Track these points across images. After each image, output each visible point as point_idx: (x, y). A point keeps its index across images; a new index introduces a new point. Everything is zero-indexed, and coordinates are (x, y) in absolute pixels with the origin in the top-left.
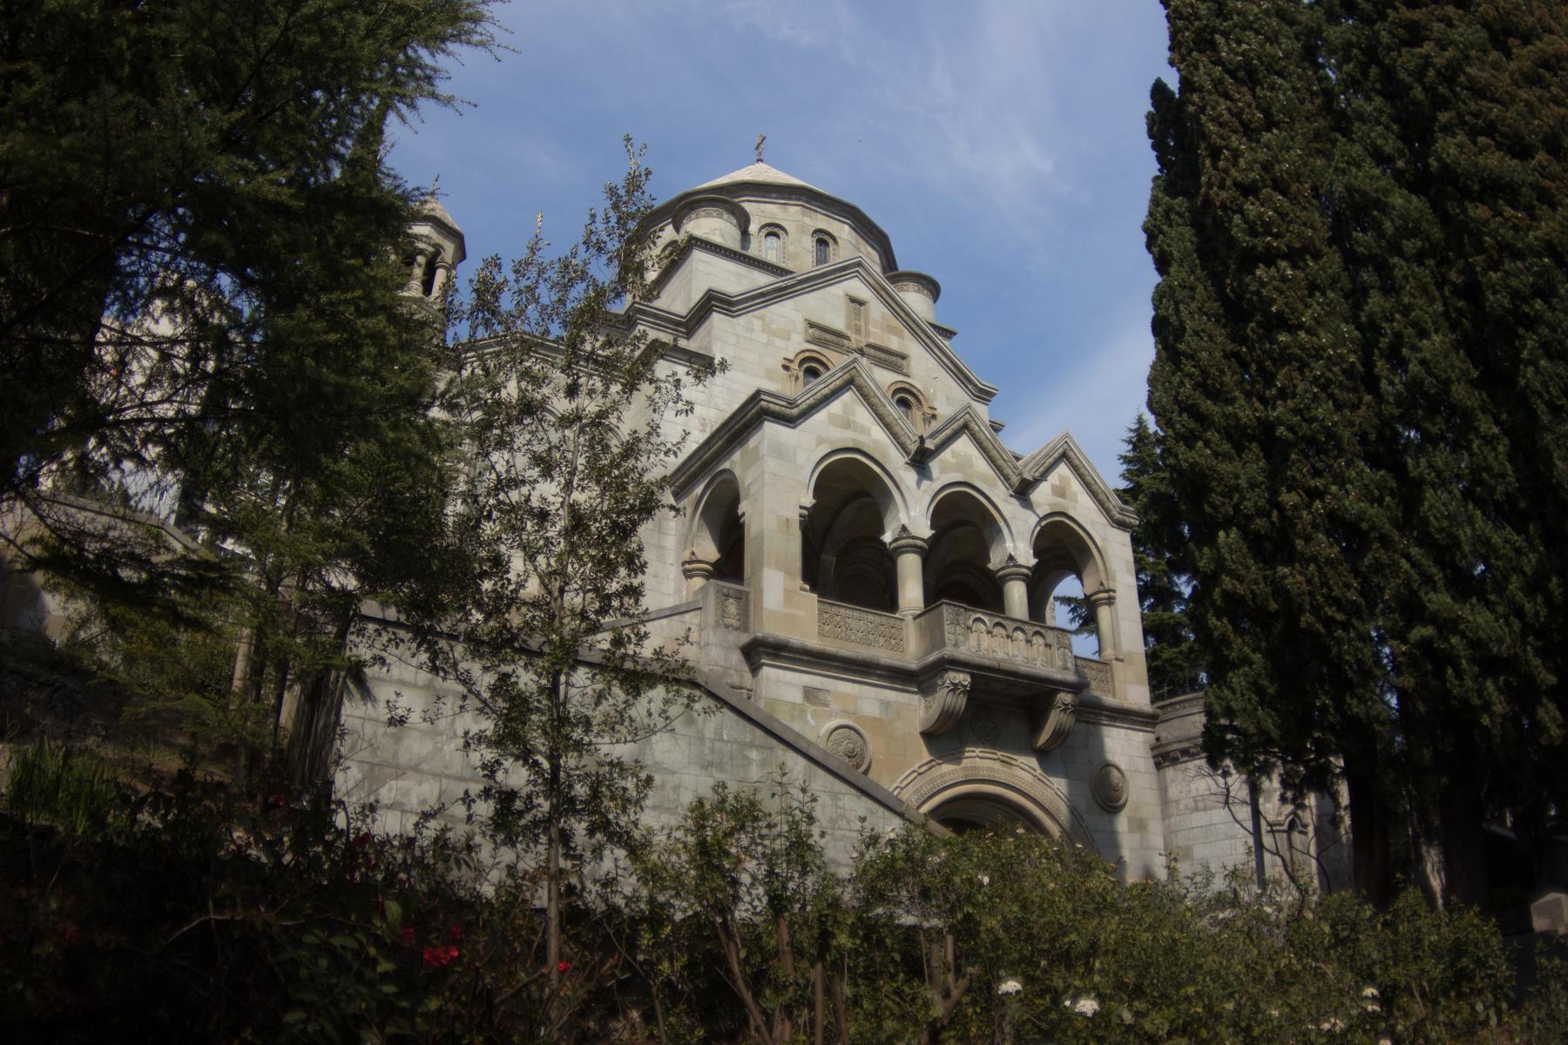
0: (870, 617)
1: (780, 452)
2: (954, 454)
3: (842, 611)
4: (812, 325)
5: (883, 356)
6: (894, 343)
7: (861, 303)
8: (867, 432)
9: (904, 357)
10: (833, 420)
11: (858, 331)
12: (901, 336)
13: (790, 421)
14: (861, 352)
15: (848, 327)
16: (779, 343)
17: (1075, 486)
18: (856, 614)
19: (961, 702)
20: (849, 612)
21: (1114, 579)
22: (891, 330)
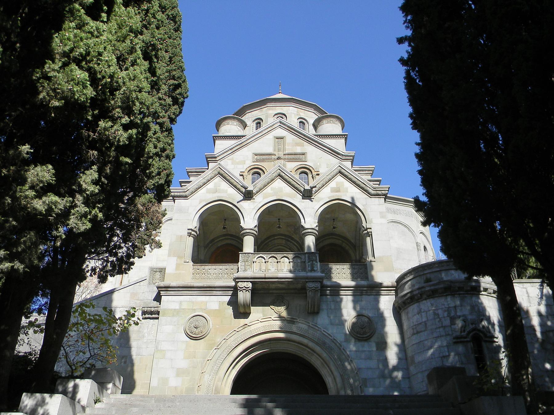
0: (221, 267)
1: (181, 210)
2: (272, 189)
3: (207, 267)
5: (293, 156)
6: (299, 150)
7: (282, 138)
8: (226, 191)
9: (304, 154)
10: (209, 191)
13: (186, 197)
16: (241, 166)
17: (347, 184)
18: (214, 267)
20: (210, 267)
21: (371, 222)
22: (297, 144)
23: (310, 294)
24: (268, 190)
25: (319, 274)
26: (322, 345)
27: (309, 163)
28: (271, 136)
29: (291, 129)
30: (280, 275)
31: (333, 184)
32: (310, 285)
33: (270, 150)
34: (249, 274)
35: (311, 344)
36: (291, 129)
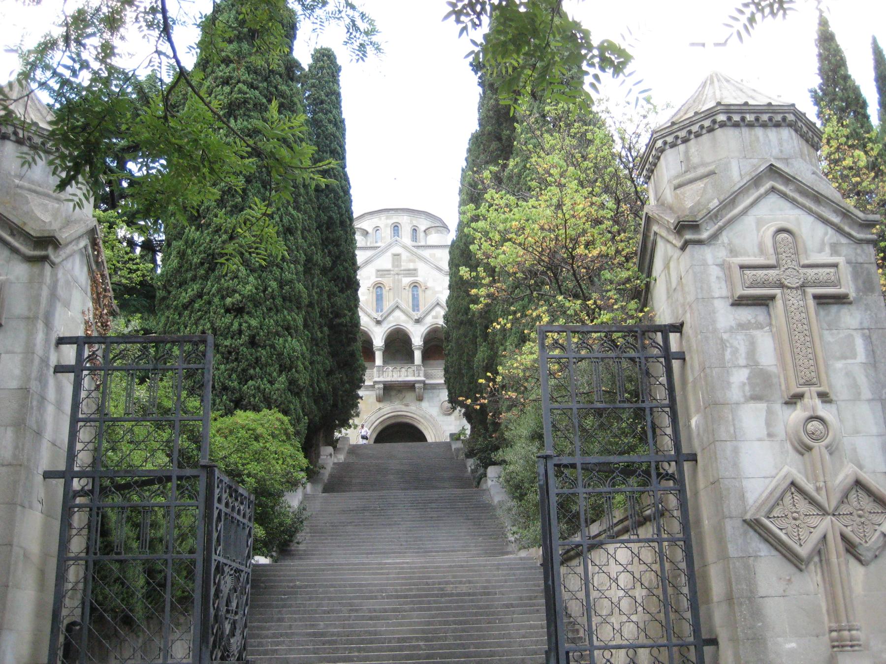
4: (378, 271)
6: (411, 266)
7: (398, 255)
9: (415, 270)
11: (397, 266)
12: (414, 261)
14: (398, 274)
15: (393, 266)
19: (382, 392)
22: (411, 261)
23: (417, 390)
24: (391, 318)
25: (422, 378)
26: (424, 418)
27: (419, 279)
28: (389, 254)
29: (405, 247)
30: (400, 379)
31: (433, 313)
32: (417, 385)
33: (389, 266)
34: (381, 379)
35: (418, 418)
36: (405, 247)
